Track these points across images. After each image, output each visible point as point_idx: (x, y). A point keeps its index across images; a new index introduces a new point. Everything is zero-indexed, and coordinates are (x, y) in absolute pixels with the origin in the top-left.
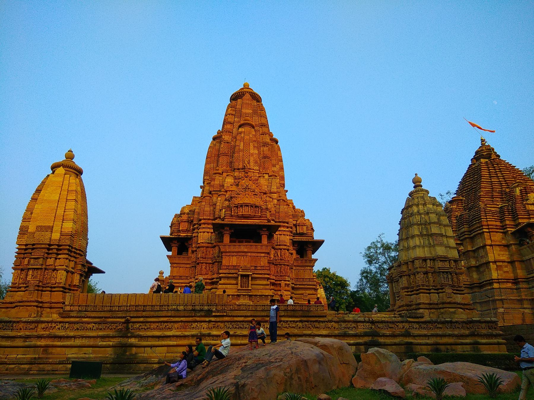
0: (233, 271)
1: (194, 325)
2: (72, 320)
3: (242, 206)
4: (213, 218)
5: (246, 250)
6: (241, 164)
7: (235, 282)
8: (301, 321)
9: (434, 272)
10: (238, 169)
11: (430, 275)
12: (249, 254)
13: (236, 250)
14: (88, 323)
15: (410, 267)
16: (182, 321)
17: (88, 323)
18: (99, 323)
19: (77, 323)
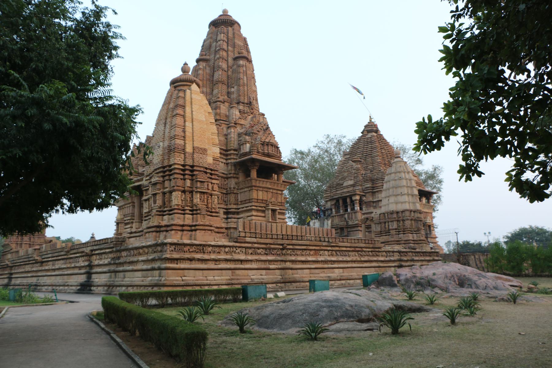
0: (262, 205)
1: (322, 252)
2: (246, 245)
3: (267, 145)
4: (225, 148)
5: (270, 187)
6: (246, 98)
7: (263, 215)
8: (371, 251)
9: (415, 220)
10: (243, 103)
11: (413, 222)
12: (271, 190)
13: (264, 186)
14: (259, 248)
15: (400, 215)
16: (315, 250)
17: (259, 248)
18: (266, 249)
19: (250, 248)
